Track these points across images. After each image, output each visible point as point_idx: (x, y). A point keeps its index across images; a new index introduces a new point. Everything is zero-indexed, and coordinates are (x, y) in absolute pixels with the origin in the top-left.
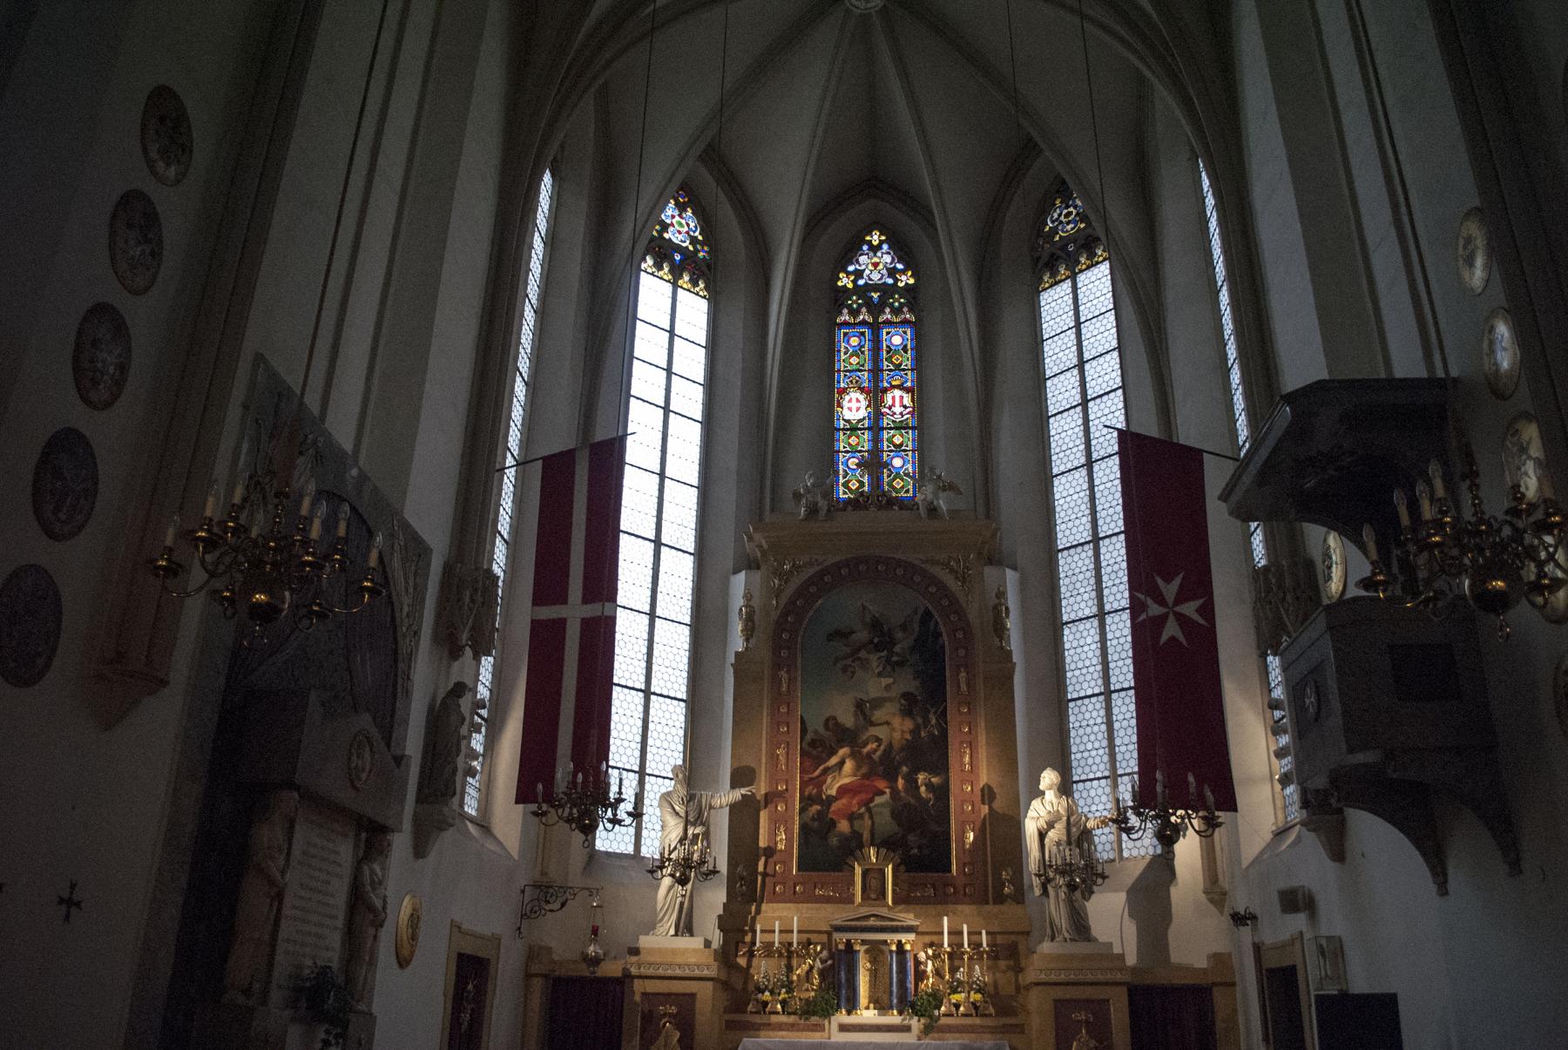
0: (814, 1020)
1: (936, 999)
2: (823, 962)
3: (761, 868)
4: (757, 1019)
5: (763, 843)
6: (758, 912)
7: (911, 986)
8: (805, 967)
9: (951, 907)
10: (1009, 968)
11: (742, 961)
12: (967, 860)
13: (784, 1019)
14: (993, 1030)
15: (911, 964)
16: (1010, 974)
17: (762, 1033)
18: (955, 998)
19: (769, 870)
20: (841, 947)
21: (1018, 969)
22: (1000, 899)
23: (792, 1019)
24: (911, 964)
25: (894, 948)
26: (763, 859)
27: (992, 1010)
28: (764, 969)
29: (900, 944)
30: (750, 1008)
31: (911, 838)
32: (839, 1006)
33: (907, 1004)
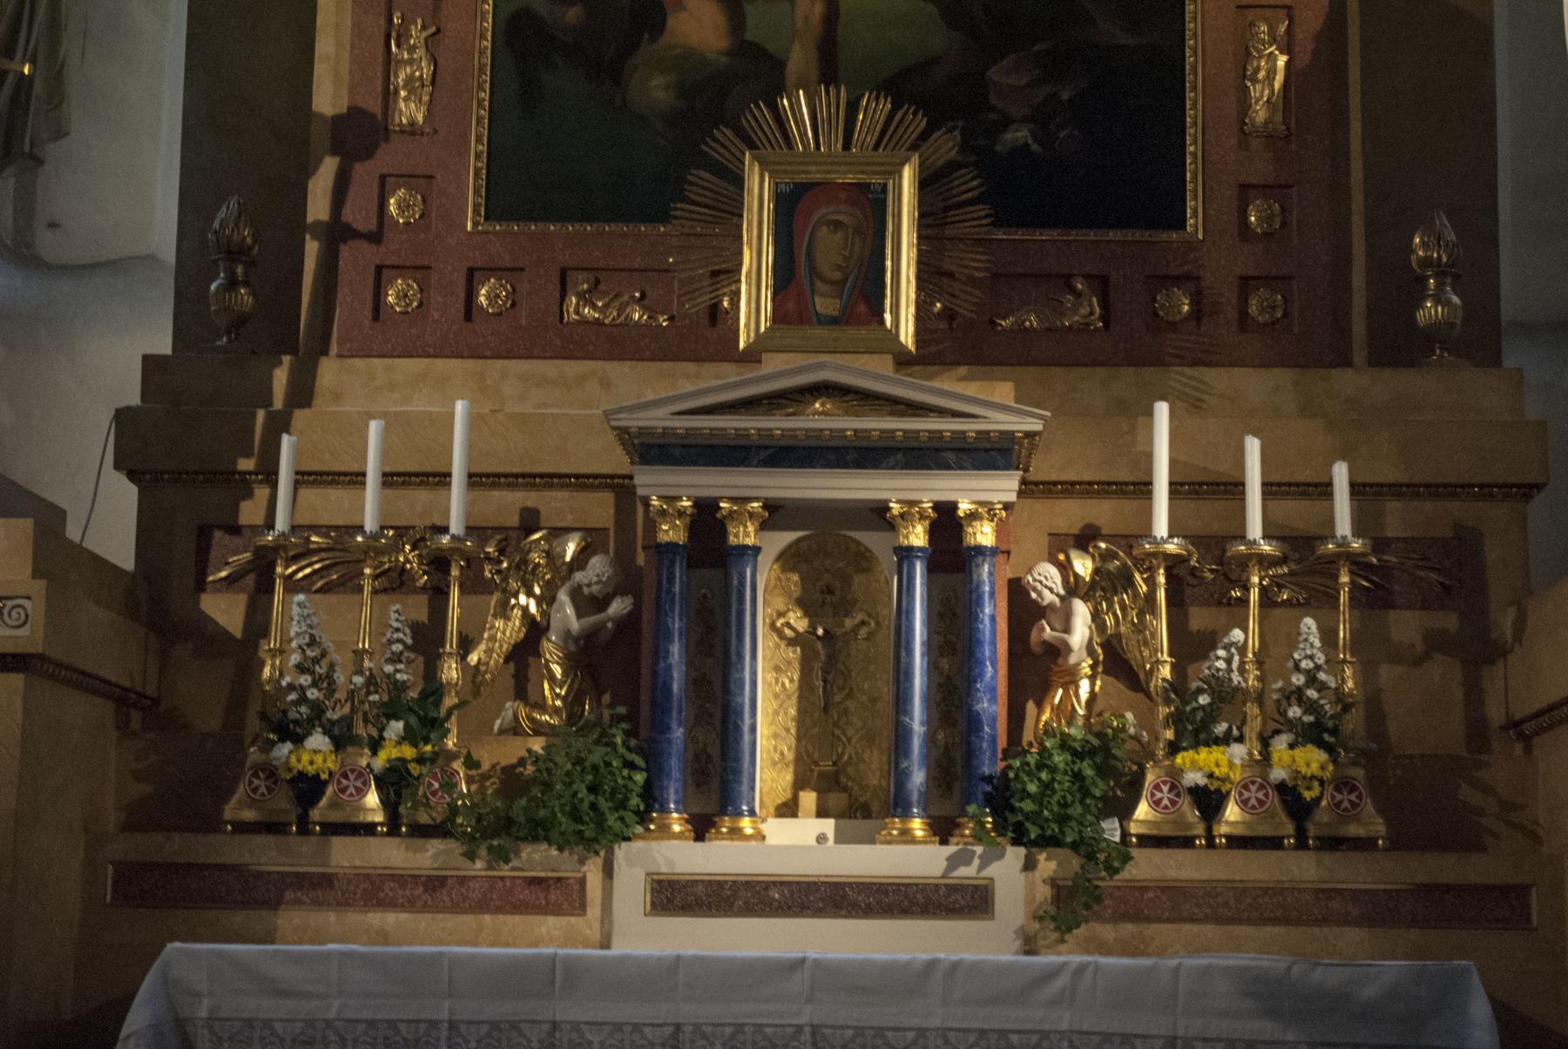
0: (537, 858)
1: (1109, 771)
2: (588, 604)
3: (318, 208)
4: (266, 855)
5: (327, 99)
6: (302, 394)
7: (992, 705)
8: (508, 631)
9: (1179, 376)
10: (1436, 643)
11: (225, 611)
12: (1260, 170)
13: (393, 854)
14: (1378, 911)
15: (993, 614)
16: (1444, 673)
17: (290, 919)
18: (1198, 764)
19: (358, 215)
20: (671, 532)
21: (1479, 651)
22: (1400, 345)
23: (428, 856)
24: (993, 614)
25: (917, 536)
26: (328, 168)
27: (1372, 824)
28: (318, 636)
29: (946, 522)
30: (237, 809)
31: (1006, 75)
32: (652, 798)
33: (977, 791)
